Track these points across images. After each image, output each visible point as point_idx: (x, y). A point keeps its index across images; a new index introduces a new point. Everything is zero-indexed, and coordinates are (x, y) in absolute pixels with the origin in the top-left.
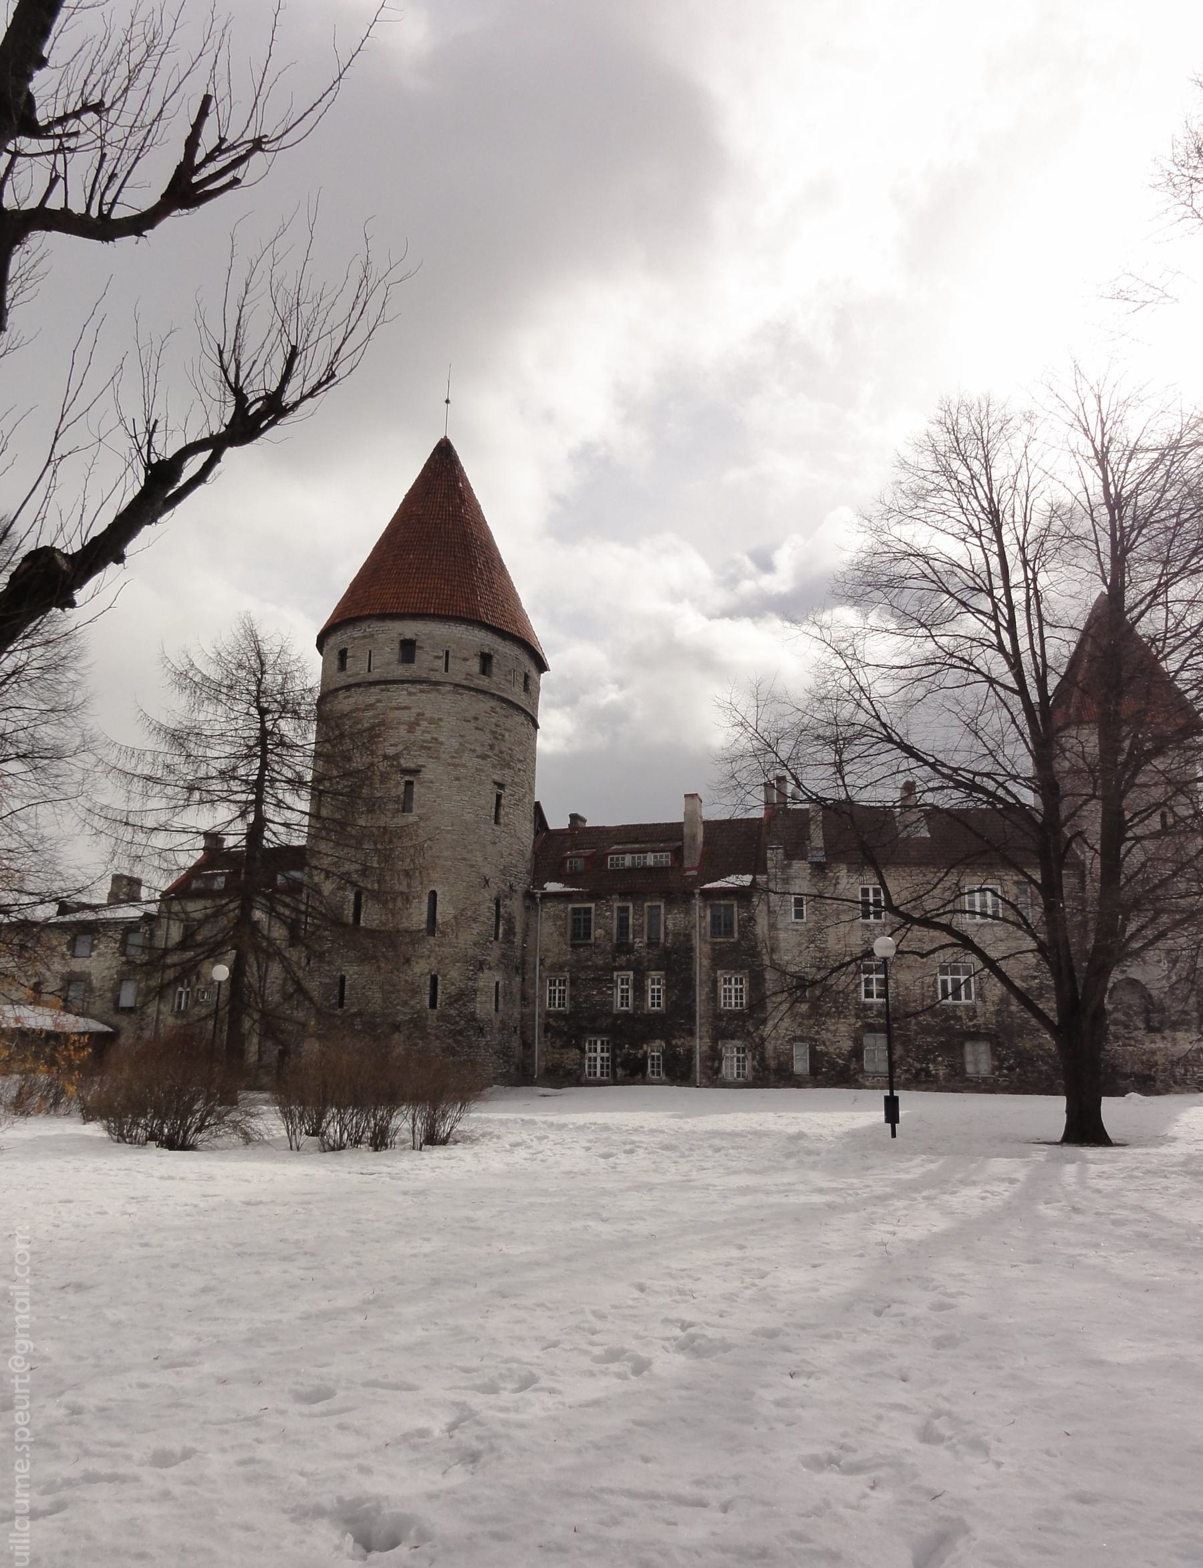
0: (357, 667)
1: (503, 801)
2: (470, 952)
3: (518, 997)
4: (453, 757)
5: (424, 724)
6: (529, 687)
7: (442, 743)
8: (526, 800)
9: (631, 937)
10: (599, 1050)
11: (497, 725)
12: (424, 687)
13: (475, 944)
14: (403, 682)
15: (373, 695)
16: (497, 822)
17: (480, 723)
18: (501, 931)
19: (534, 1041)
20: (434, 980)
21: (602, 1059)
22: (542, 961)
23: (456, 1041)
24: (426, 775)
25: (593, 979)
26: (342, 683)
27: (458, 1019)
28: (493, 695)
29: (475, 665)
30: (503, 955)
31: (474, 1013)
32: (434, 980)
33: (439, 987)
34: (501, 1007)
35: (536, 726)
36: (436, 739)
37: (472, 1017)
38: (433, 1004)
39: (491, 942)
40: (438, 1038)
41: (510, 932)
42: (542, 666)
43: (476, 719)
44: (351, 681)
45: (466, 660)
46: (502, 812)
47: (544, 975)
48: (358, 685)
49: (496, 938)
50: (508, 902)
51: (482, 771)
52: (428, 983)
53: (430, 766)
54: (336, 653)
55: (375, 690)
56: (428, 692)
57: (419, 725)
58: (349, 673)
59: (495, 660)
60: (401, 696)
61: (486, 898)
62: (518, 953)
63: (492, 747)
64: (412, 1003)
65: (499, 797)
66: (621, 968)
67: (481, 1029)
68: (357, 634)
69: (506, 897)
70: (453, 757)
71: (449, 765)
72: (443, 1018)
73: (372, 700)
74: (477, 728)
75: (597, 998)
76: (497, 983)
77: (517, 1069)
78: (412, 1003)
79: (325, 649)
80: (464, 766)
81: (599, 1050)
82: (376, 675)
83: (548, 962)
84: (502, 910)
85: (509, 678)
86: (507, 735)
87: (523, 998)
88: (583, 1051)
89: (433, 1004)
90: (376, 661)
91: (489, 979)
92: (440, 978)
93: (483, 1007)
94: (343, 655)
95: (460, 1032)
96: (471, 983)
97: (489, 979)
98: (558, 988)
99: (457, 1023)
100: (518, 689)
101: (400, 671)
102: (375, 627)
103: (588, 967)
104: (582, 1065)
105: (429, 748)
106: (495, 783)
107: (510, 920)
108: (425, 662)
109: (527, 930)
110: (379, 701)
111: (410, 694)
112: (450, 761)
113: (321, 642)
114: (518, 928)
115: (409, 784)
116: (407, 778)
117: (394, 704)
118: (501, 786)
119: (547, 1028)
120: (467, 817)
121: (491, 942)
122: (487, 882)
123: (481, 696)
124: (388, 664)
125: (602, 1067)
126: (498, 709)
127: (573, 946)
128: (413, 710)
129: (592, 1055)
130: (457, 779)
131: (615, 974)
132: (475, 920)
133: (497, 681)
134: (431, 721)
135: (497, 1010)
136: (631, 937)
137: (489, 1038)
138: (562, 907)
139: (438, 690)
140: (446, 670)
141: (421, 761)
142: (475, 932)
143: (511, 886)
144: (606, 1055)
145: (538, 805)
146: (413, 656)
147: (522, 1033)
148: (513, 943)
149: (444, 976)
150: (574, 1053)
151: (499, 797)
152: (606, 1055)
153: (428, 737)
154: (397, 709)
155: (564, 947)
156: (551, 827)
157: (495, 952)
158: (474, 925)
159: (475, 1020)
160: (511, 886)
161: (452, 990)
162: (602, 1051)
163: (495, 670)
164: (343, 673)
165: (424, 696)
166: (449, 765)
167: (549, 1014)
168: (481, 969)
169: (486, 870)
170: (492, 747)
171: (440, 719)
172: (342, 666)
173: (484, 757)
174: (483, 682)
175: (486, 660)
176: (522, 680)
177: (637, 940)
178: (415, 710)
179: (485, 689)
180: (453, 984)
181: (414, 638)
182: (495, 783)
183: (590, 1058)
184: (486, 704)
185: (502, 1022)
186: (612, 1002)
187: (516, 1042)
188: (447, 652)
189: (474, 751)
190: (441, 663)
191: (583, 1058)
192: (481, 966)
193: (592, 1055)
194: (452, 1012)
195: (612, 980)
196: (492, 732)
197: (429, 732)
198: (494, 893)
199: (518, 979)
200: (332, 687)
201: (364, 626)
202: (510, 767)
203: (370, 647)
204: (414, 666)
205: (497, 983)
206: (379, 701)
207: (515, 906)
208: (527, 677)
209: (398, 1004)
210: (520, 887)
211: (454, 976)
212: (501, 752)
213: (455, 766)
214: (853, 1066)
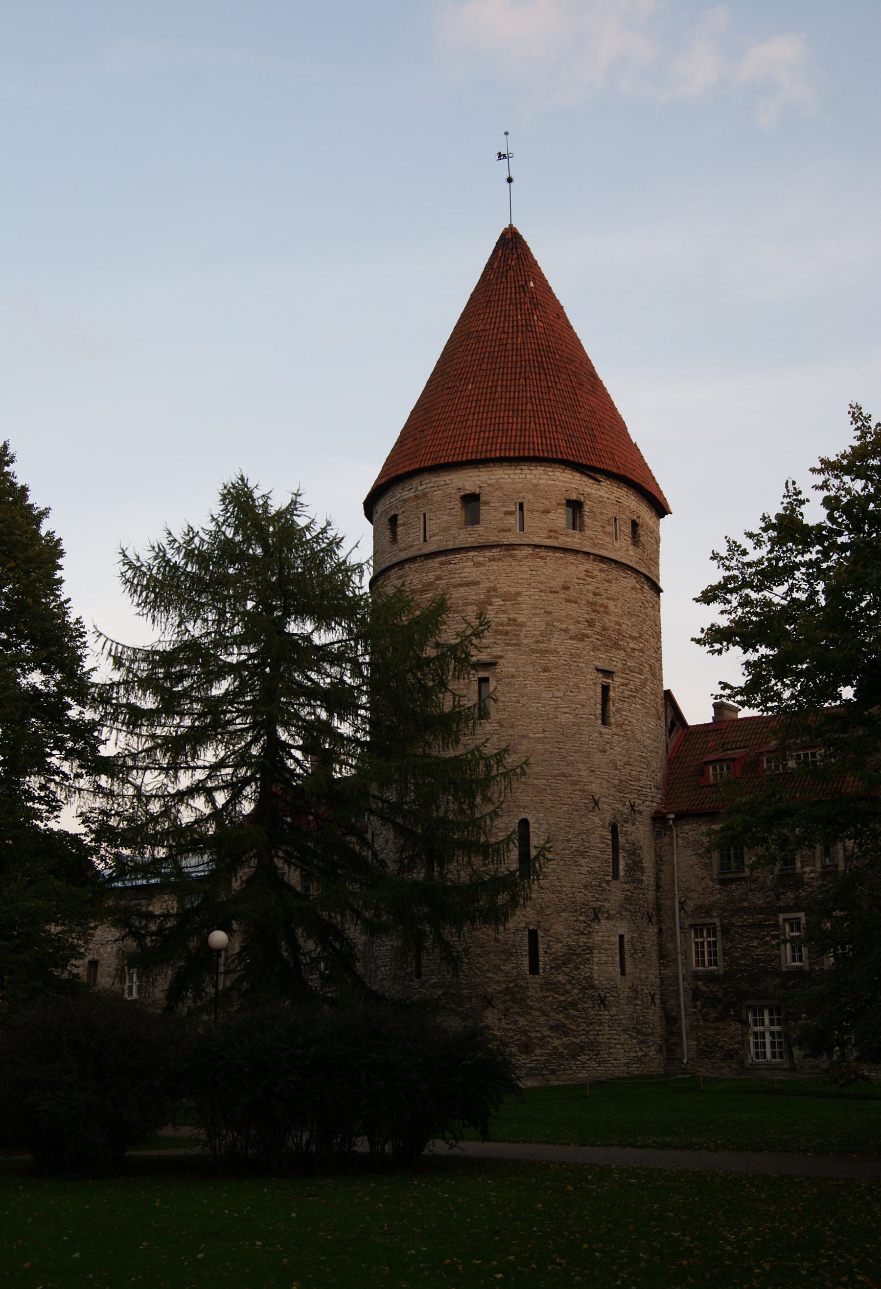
0: (412, 539)
1: (612, 694)
2: (579, 897)
3: (654, 955)
4: (537, 642)
5: (498, 602)
6: (642, 538)
7: (522, 625)
8: (648, 690)
9: (799, 865)
10: (767, 1022)
11: (595, 594)
12: (495, 552)
13: (585, 887)
14: (467, 549)
15: (432, 570)
16: (605, 721)
17: (572, 594)
18: (622, 866)
19: (679, 1012)
20: (533, 935)
21: (772, 1034)
22: (682, 904)
23: (567, 1016)
24: (505, 667)
25: (751, 926)
26: (395, 560)
27: (568, 987)
28: (588, 554)
29: (560, 518)
30: (628, 899)
31: (591, 977)
32: (533, 935)
33: (541, 946)
34: (629, 968)
35: (659, 591)
36: (515, 620)
37: (589, 984)
38: (534, 968)
39: (608, 883)
40: (544, 1014)
41: (636, 866)
42: (661, 509)
43: (566, 588)
44: (404, 555)
45: (547, 512)
46: (612, 708)
47: (688, 922)
48: (413, 560)
49: (616, 876)
50: (629, 828)
51: (579, 656)
52: (526, 940)
53: (510, 655)
54: (385, 520)
55: (434, 563)
56: (500, 559)
57: (490, 604)
58: (402, 546)
59: (586, 508)
60: (467, 568)
61: (598, 822)
62: (651, 895)
63: (590, 623)
64: (507, 968)
65: (605, 689)
66: (788, 909)
67: (603, 1001)
68: (408, 495)
69: (626, 821)
70: (537, 642)
71: (533, 651)
72: (549, 986)
73: (431, 576)
74: (568, 601)
75: (759, 951)
76: (621, 937)
77: (660, 1051)
78: (507, 968)
79: (375, 518)
80: (555, 652)
81: (767, 1022)
82: (431, 548)
83: (691, 905)
84: (621, 840)
85: (610, 529)
86: (611, 604)
87: (662, 956)
88: (745, 1023)
89: (534, 968)
90: (432, 527)
91: (608, 932)
92: (540, 934)
93: (604, 969)
94: (393, 520)
95: (574, 1005)
96: (583, 939)
97: (608, 932)
98: (707, 939)
99: (567, 992)
100: (625, 541)
101: (465, 537)
102: (428, 483)
103: (743, 909)
104: (744, 1043)
105: (506, 633)
106: (598, 670)
107: (634, 852)
108: (494, 520)
109: (659, 860)
110: (439, 578)
111: (478, 565)
112: (534, 646)
113: (370, 506)
114: (648, 861)
115: (484, 681)
116: (482, 674)
117: (457, 580)
118: (608, 673)
119: (696, 994)
120: (563, 718)
121: (608, 883)
122: (596, 803)
123: (571, 558)
124: (447, 529)
125: (773, 1045)
126: (596, 573)
127: (722, 882)
128: (482, 586)
129: (759, 1029)
130: (546, 670)
131: (781, 917)
132: (583, 855)
133: (595, 536)
134: (506, 598)
135: (623, 972)
136: (799, 865)
137: (614, 1011)
138: (704, 829)
139: (513, 557)
140: (522, 528)
141: (497, 651)
142: (584, 870)
143: (632, 806)
144: (776, 1028)
145: (668, 693)
146: (478, 515)
147: (663, 1002)
148: (641, 881)
149: (546, 930)
150: (734, 1027)
151: (605, 689)
152: (776, 1028)
153: (504, 618)
154: (461, 586)
155: (711, 884)
156: (691, 722)
157: (616, 894)
158: (582, 861)
159: (593, 987)
160: (632, 806)
161: (558, 948)
162: (772, 1024)
163: (587, 521)
164: (395, 548)
165: (495, 566)
166: (533, 651)
167: (696, 976)
168: (596, 918)
169: (594, 788)
170: (590, 623)
171: (518, 594)
172: (394, 540)
173: (581, 638)
174: (573, 540)
175: (575, 506)
176: (627, 530)
177: (807, 869)
178: (485, 585)
179: (576, 547)
180: (558, 941)
181: (478, 492)
182: (598, 670)
183: (756, 1034)
184: (579, 568)
185: (633, 989)
186: (779, 957)
187: (654, 1015)
188: (521, 506)
189: (566, 631)
190: (513, 521)
191: (745, 1034)
192: (597, 915)
193: (759, 1029)
194: (561, 978)
195: (776, 926)
196: (590, 604)
197: (505, 612)
198: (608, 817)
199: (653, 930)
200: (383, 566)
201: (415, 483)
202: (616, 646)
203: (424, 510)
204: (479, 528)
205: (621, 937)
206: (439, 578)
207: (640, 832)
208: (635, 525)
209: (488, 971)
210: (648, 807)
211: (560, 933)
212: (604, 629)
213: (543, 652)
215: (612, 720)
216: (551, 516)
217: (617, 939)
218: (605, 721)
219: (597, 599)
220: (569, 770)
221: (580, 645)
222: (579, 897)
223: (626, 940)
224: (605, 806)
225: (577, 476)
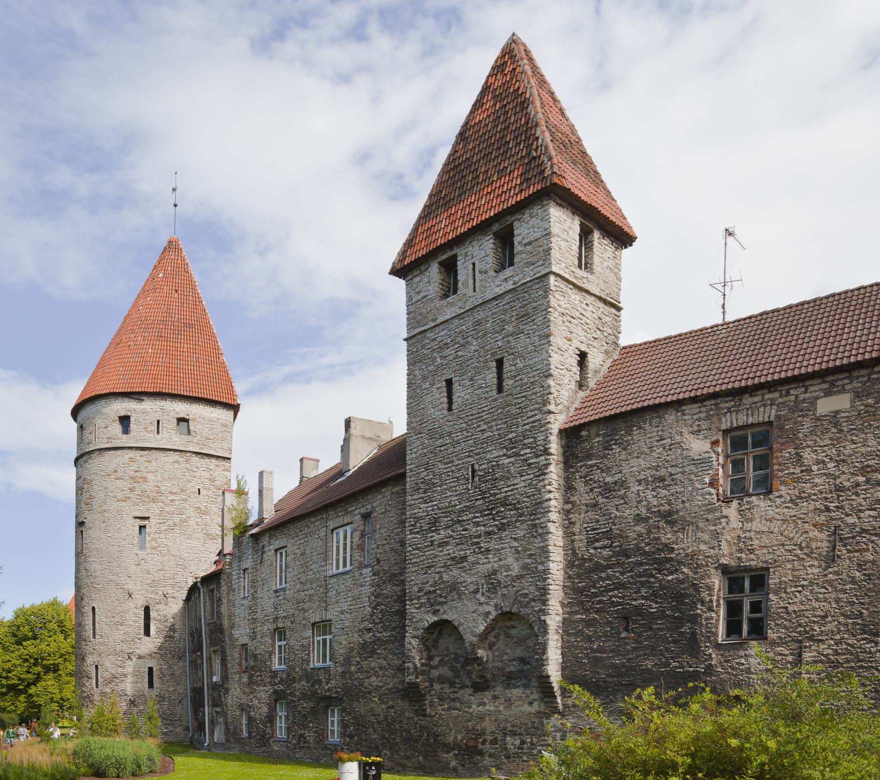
16: (142, 547)
17: (119, 474)
18: (153, 629)
28: (131, 448)
43: (116, 472)
65: (142, 528)
123: (119, 452)
175: (125, 421)
182: (136, 518)
196: (133, 478)
214: (268, 730)
215: (147, 545)
216: (109, 428)
217: (147, 669)
218: (142, 547)
219: (138, 474)
220: (114, 578)
221: (124, 504)
222: (118, 648)
223: (154, 670)
224: (138, 596)
225: (126, 399)
